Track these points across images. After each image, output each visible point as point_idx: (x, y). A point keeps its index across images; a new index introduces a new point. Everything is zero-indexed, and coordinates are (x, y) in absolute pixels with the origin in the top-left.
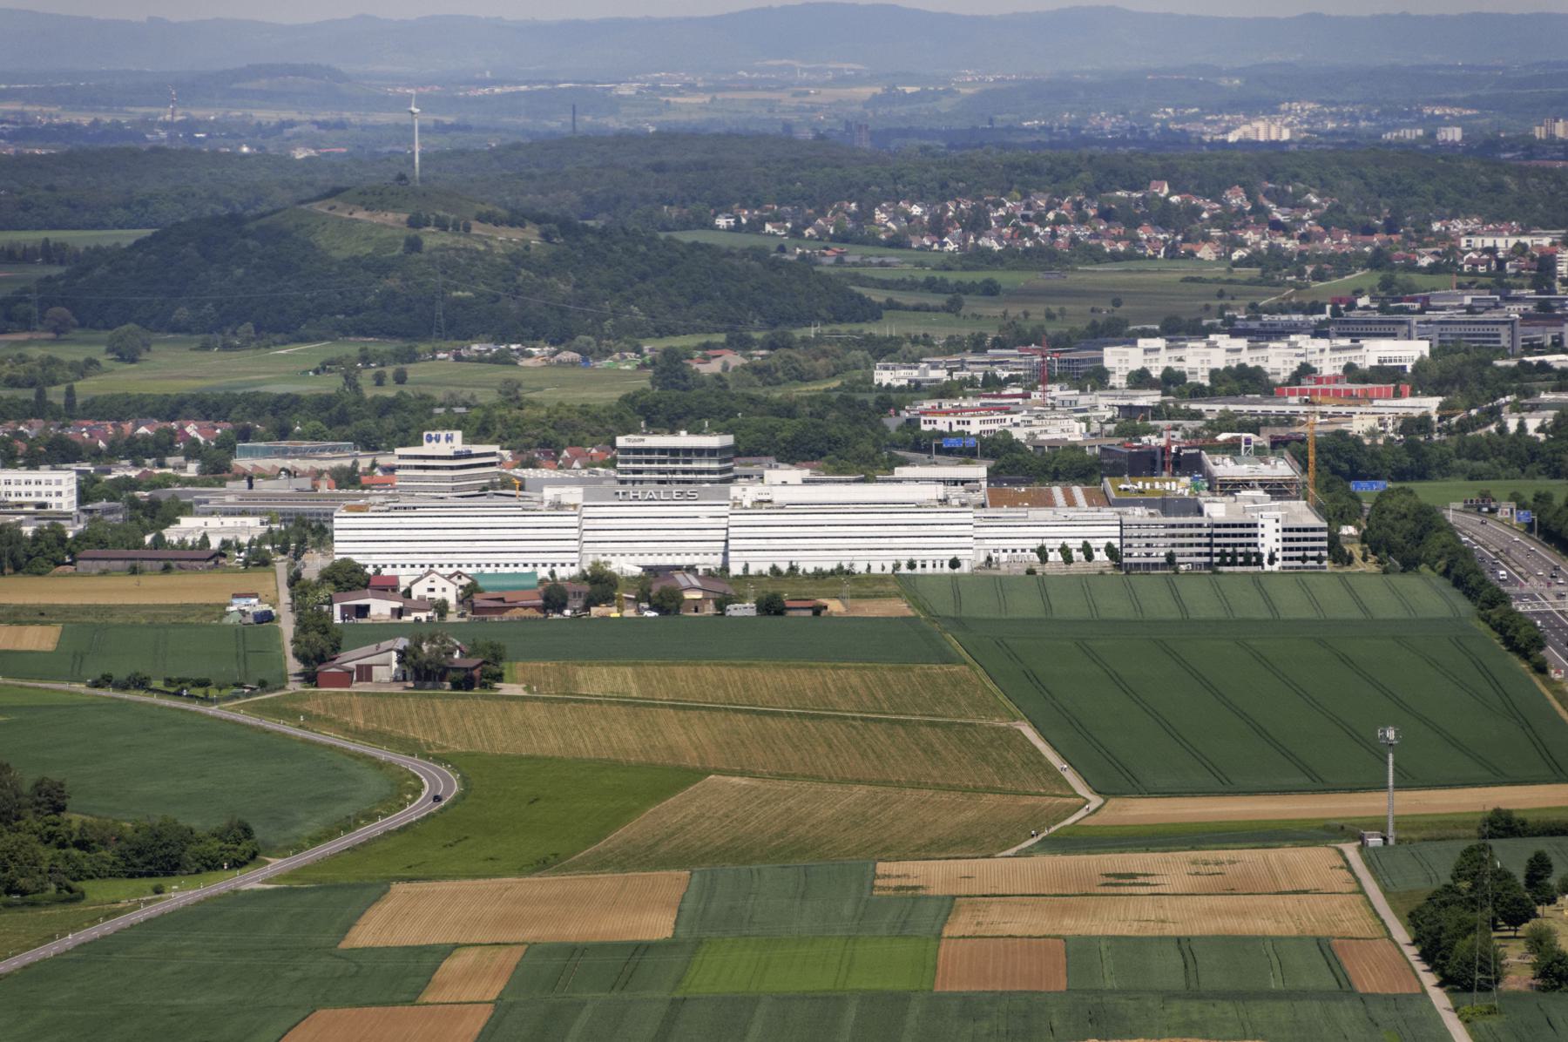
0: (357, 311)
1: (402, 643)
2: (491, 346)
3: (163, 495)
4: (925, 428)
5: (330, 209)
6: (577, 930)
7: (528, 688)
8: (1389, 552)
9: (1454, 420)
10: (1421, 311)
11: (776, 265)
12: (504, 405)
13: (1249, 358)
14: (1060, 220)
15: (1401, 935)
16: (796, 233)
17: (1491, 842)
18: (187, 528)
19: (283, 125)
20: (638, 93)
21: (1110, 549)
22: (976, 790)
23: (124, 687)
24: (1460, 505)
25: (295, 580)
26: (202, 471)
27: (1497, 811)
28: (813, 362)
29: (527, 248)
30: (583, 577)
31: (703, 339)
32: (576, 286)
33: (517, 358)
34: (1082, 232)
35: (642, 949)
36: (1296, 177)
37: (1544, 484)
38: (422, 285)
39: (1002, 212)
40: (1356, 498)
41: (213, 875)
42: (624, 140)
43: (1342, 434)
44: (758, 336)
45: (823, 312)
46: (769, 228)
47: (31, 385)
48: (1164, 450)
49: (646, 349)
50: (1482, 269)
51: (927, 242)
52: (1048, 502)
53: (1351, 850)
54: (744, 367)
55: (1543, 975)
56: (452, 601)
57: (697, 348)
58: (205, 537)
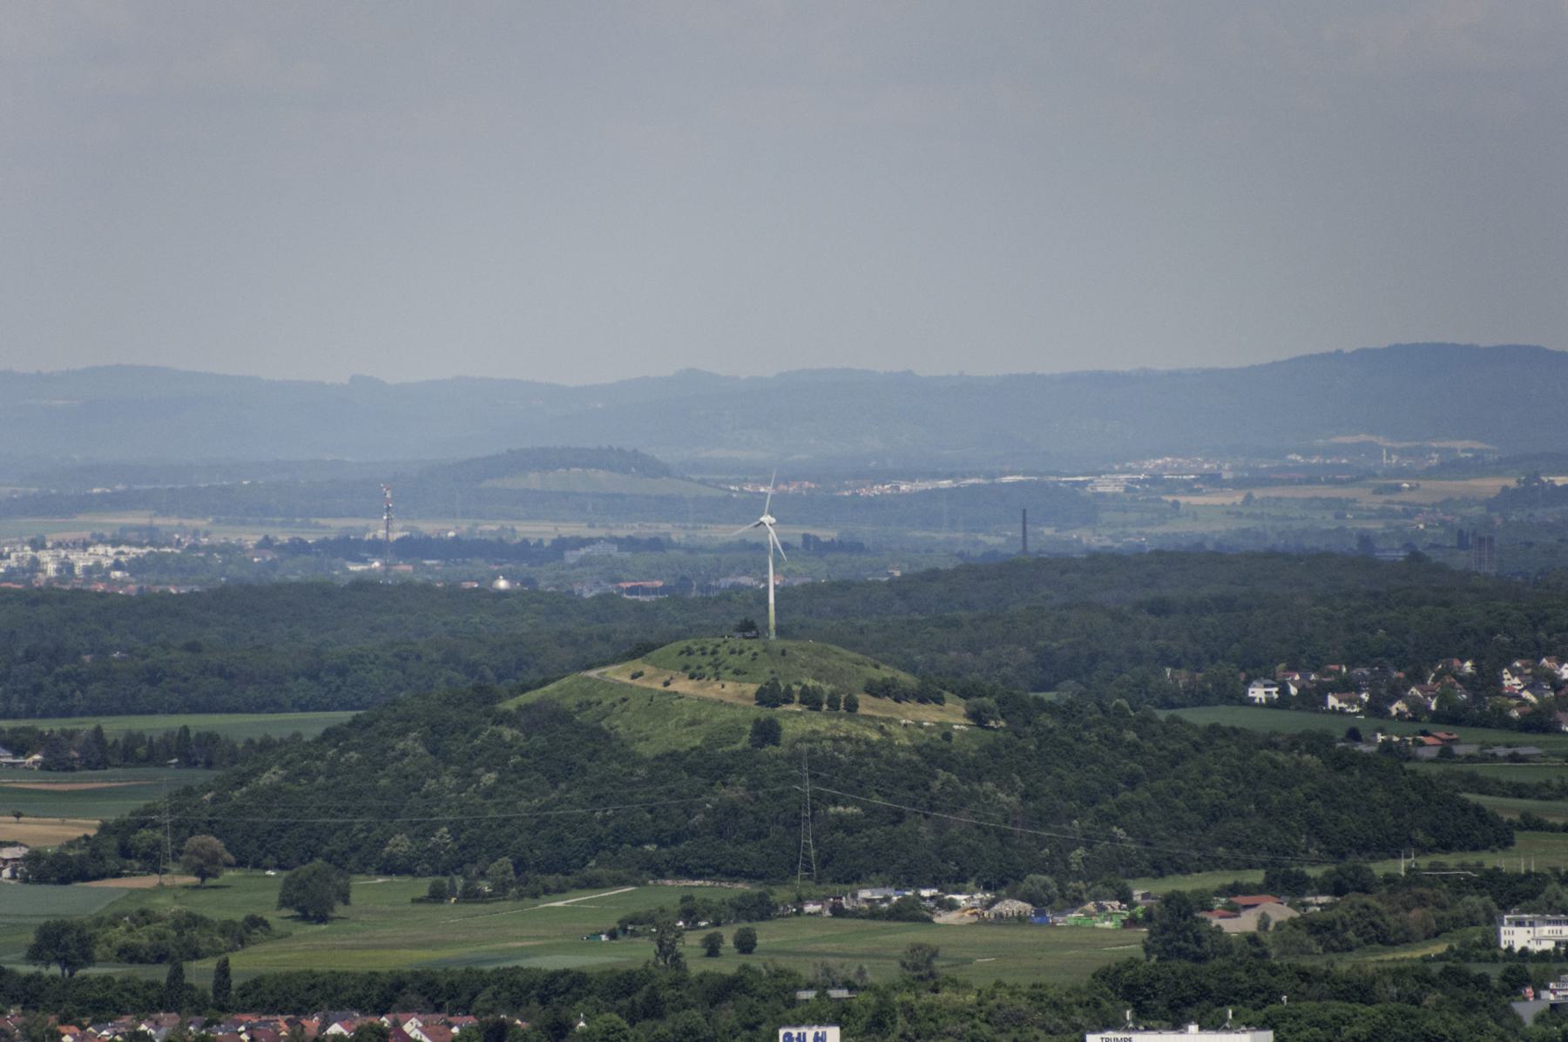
0: (676, 840)
2: (890, 892)
5: (634, 677)
11: (1342, 762)
12: (910, 986)
16: (1376, 709)
19: (561, 545)
20: (1127, 490)
28: (1402, 913)
29: (947, 737)
31: (1228, 878)
32: (1026, 796)
33: (931, 911)
38: (777, 797)
42: (1099, 563)
44: (1314, 872)
45: (1420, 836)
46: (1332, 701)
47: (160, 959)
49: (1137, 895)
54: (1293, 923)
57: (1219, 893)
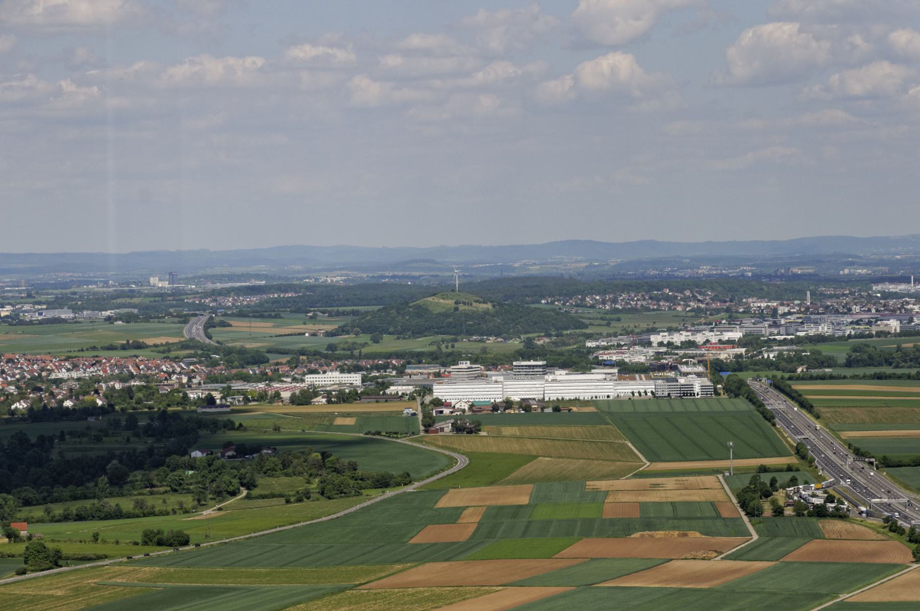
0: (440, 328)
1: (452, 421)
3: (386, 380)
4: (600, 358)
6: (501, 502)
7: (488, 433)
8: (731, 392)
9: (749, 355)
10: (740, 324)
11: (558, 314)
13: (691, 338)
14: (638, 300)
15: (735, 501)
16: (564, 304)
17: (761, 474)
18: (392, 389)
19: (420, 276)
21: (652, 392)
22: (615, 460)
23: (374, 434)
24: (751, 379)
25: (422, 404)
26: (397, 373)
27: (762, 465)
29: (488, 310)
30: (504, 402)
31: (538, 334)
32: (502, 320)
34: (644, 303)
35: (520, 507)
36: (704, 287)
37: (775, 373)
38: (458, 320)
39: (622, 298)
40: (721, 377)
41: (399, 487)
42: (515, 279)
43: (718, 359)
44: (553, 333)
45: (572, 327)
46: (556, 303)
47: (349, 350)
48: (668, 364)
50: (757, 312)
51: (601, 306)
52: (634, 379)
53: (720, 477)
55: (775, 512)
56: (467, 409)
58: (397, 392)
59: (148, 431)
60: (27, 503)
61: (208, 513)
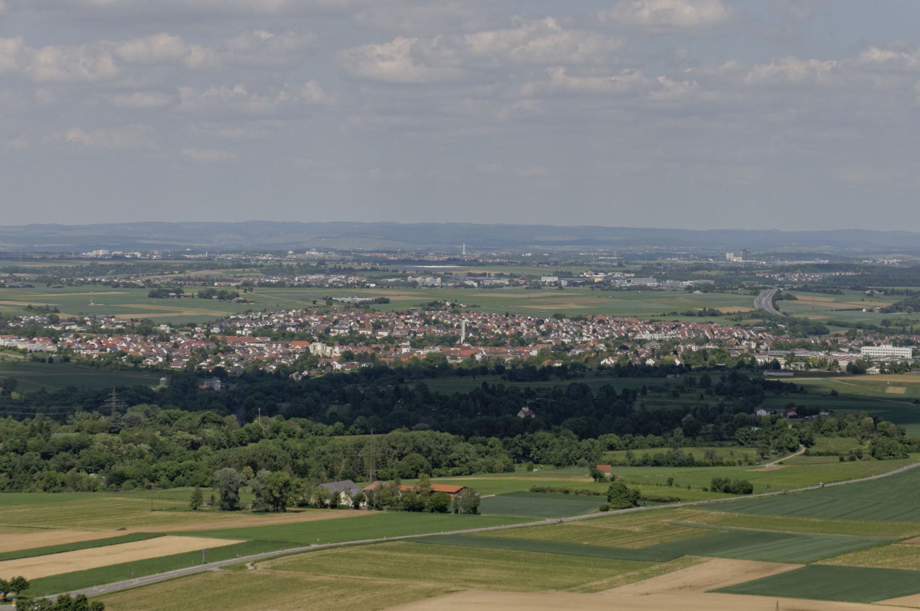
47: (902, 325)
59: (720, 390)
60: (611, 447)
61: (769, 466)
